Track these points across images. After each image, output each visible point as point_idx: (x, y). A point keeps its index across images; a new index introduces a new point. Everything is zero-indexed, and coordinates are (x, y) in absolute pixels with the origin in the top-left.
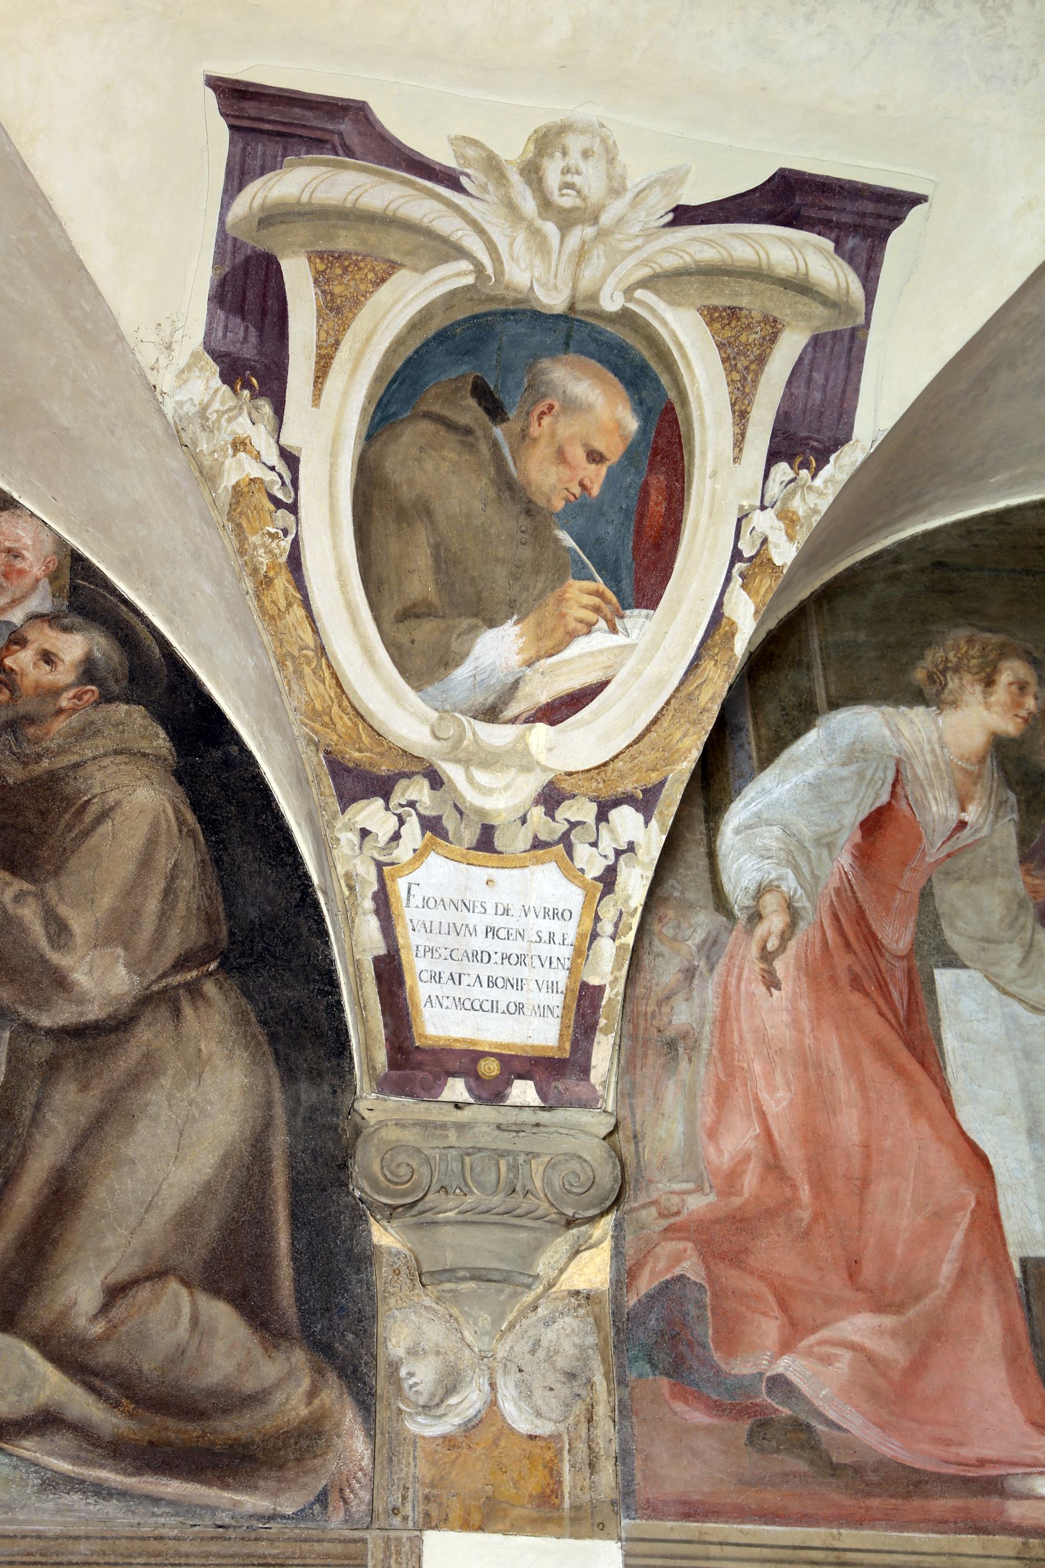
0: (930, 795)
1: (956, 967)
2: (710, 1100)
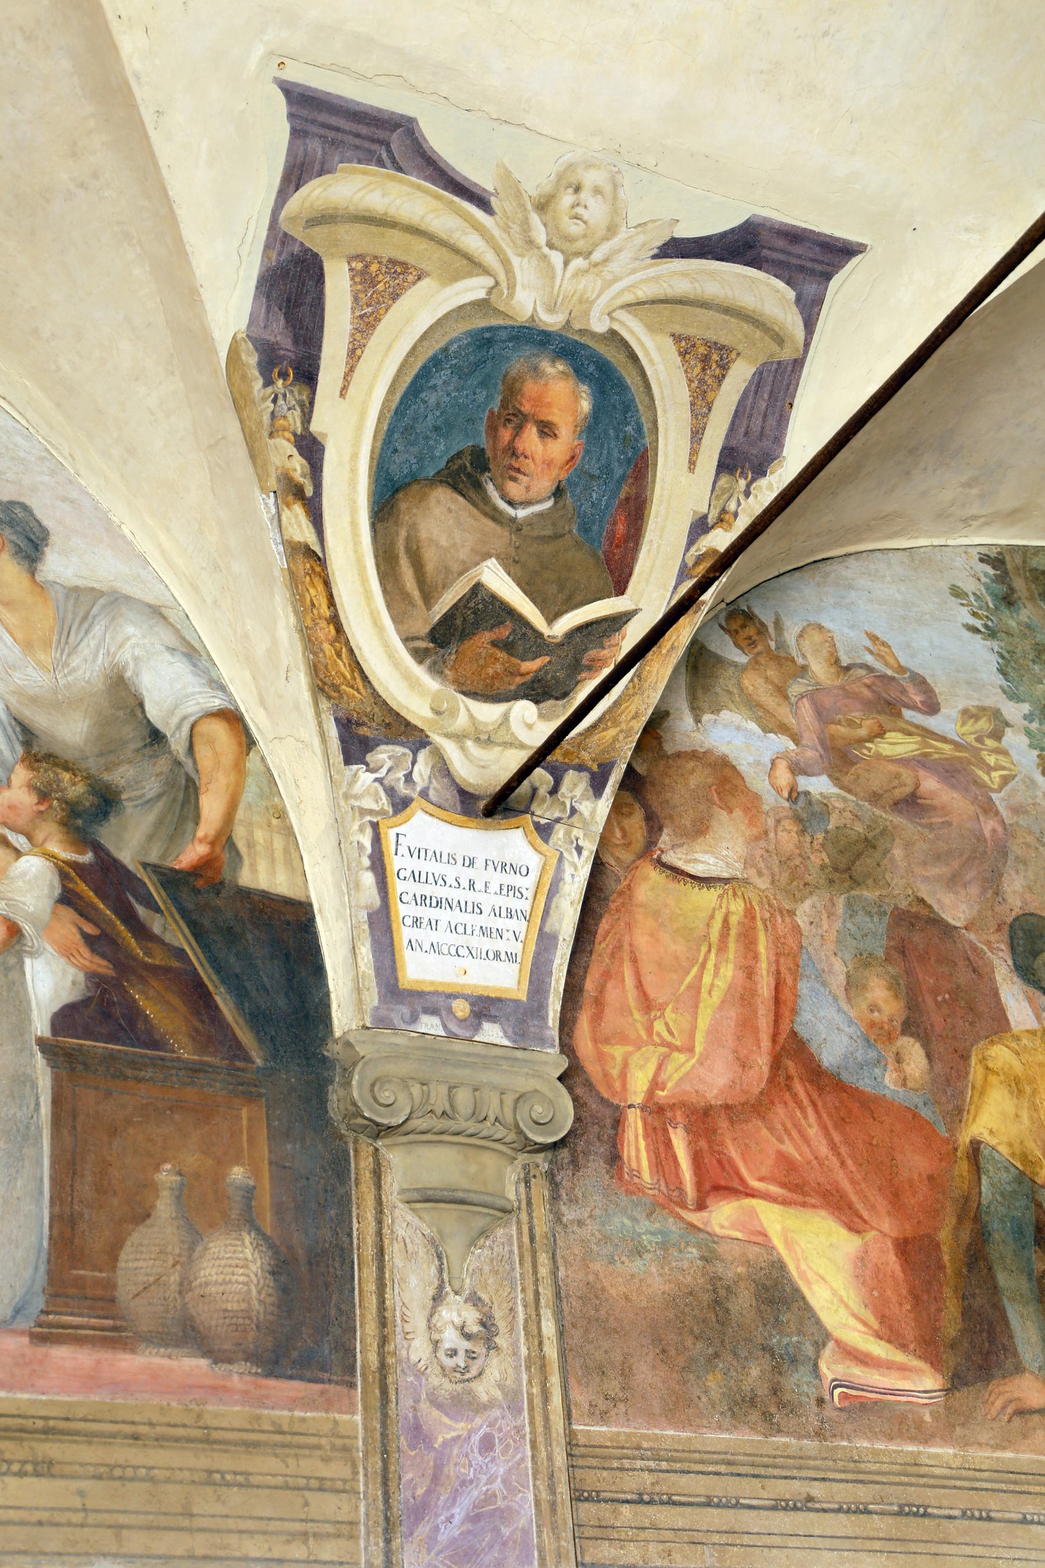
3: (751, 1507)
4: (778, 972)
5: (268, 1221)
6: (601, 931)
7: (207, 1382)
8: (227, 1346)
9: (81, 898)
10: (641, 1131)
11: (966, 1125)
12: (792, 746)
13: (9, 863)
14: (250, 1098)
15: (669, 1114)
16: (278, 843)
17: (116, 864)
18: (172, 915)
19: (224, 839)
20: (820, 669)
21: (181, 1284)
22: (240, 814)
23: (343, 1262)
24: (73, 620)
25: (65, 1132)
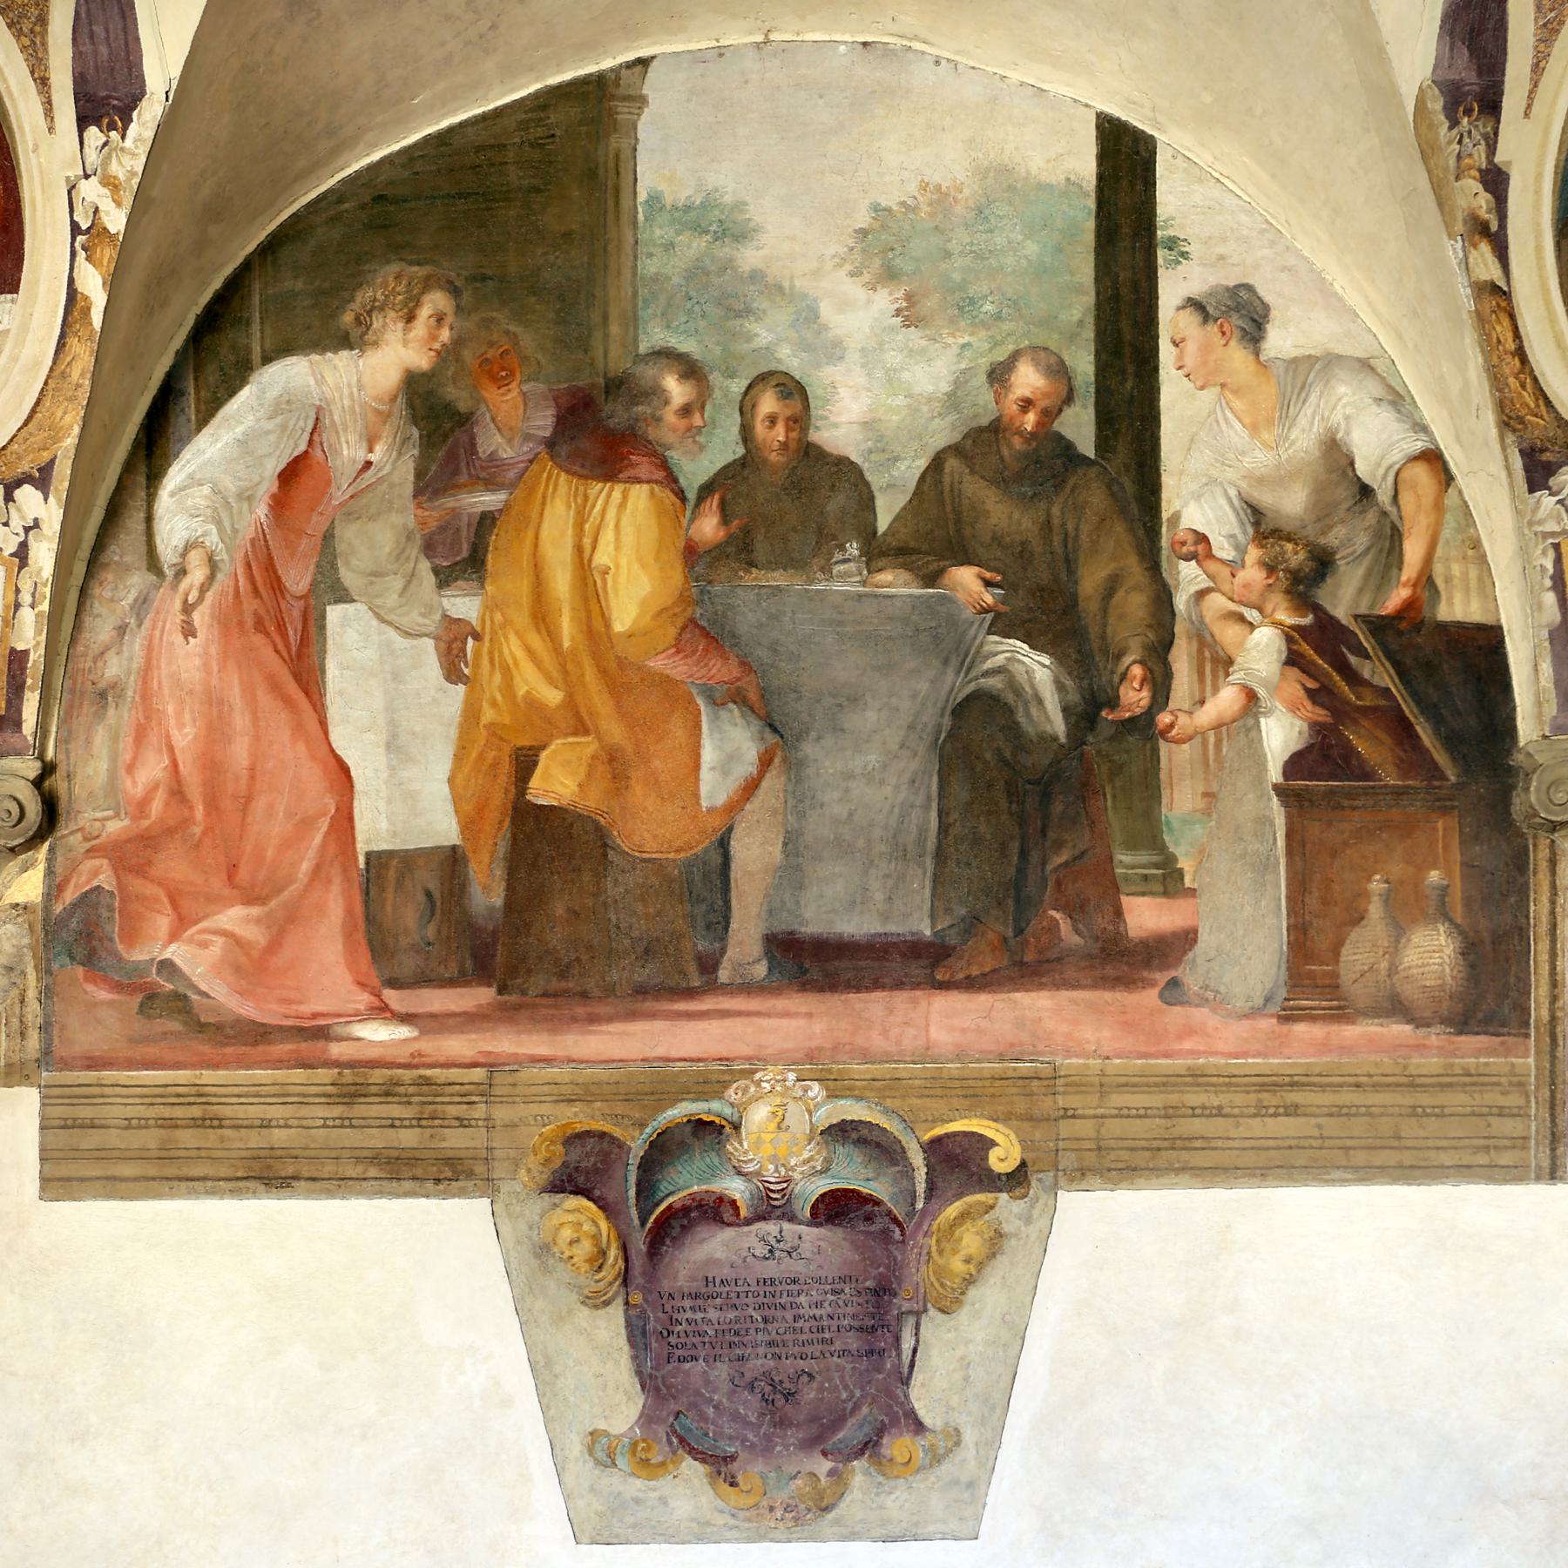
0: (343, 439)
1: (345, 602)
2: (130, 740)
5: (1458, 914)
7: (1412, 1042)
8: (1427, 1014)
9: (1302, 656)
13: (1245, 637)
14: (1444, 811)
16: (1473, 573)
17: (1333, 621)
18: (1380, 661)
19: (1425, 579)
21: (1390, 969)
22: (1439, 552)
23: (1521, 940)
24: (1292, 392)
25: (1297, 858)
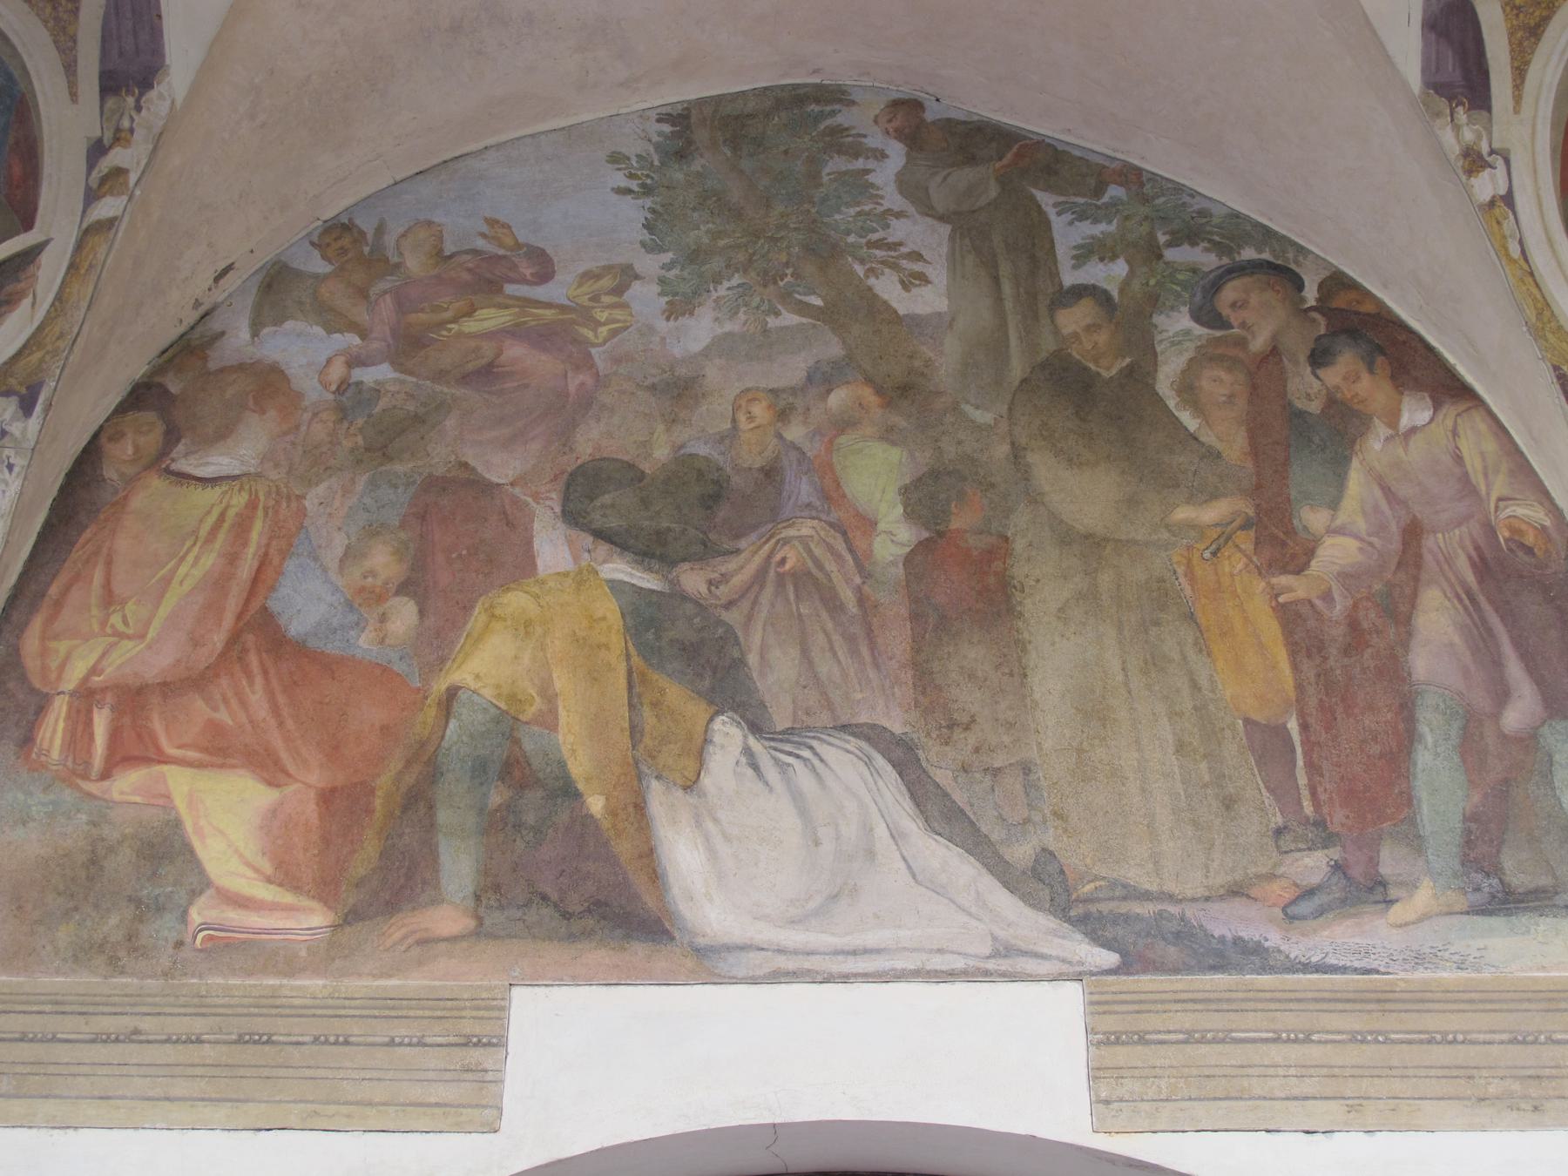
3: (67, 1041)
4: (266, 554)
6: (82, 541)
10: (63, 715)
11: (447, 673)
12: (356, 340)
15: (98, 697)
20: (414, 264)
